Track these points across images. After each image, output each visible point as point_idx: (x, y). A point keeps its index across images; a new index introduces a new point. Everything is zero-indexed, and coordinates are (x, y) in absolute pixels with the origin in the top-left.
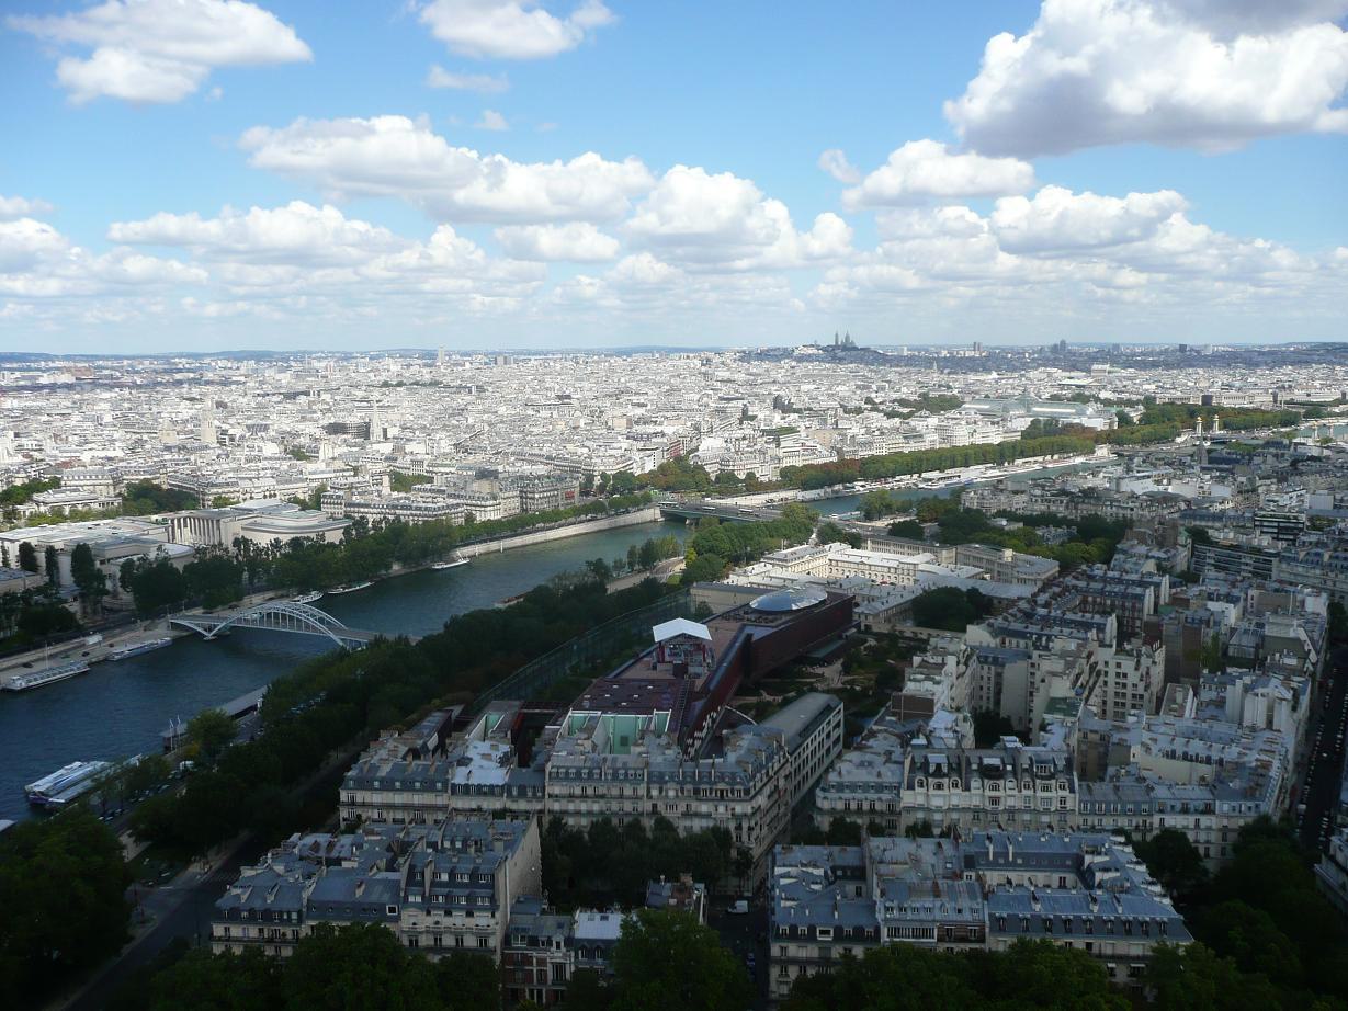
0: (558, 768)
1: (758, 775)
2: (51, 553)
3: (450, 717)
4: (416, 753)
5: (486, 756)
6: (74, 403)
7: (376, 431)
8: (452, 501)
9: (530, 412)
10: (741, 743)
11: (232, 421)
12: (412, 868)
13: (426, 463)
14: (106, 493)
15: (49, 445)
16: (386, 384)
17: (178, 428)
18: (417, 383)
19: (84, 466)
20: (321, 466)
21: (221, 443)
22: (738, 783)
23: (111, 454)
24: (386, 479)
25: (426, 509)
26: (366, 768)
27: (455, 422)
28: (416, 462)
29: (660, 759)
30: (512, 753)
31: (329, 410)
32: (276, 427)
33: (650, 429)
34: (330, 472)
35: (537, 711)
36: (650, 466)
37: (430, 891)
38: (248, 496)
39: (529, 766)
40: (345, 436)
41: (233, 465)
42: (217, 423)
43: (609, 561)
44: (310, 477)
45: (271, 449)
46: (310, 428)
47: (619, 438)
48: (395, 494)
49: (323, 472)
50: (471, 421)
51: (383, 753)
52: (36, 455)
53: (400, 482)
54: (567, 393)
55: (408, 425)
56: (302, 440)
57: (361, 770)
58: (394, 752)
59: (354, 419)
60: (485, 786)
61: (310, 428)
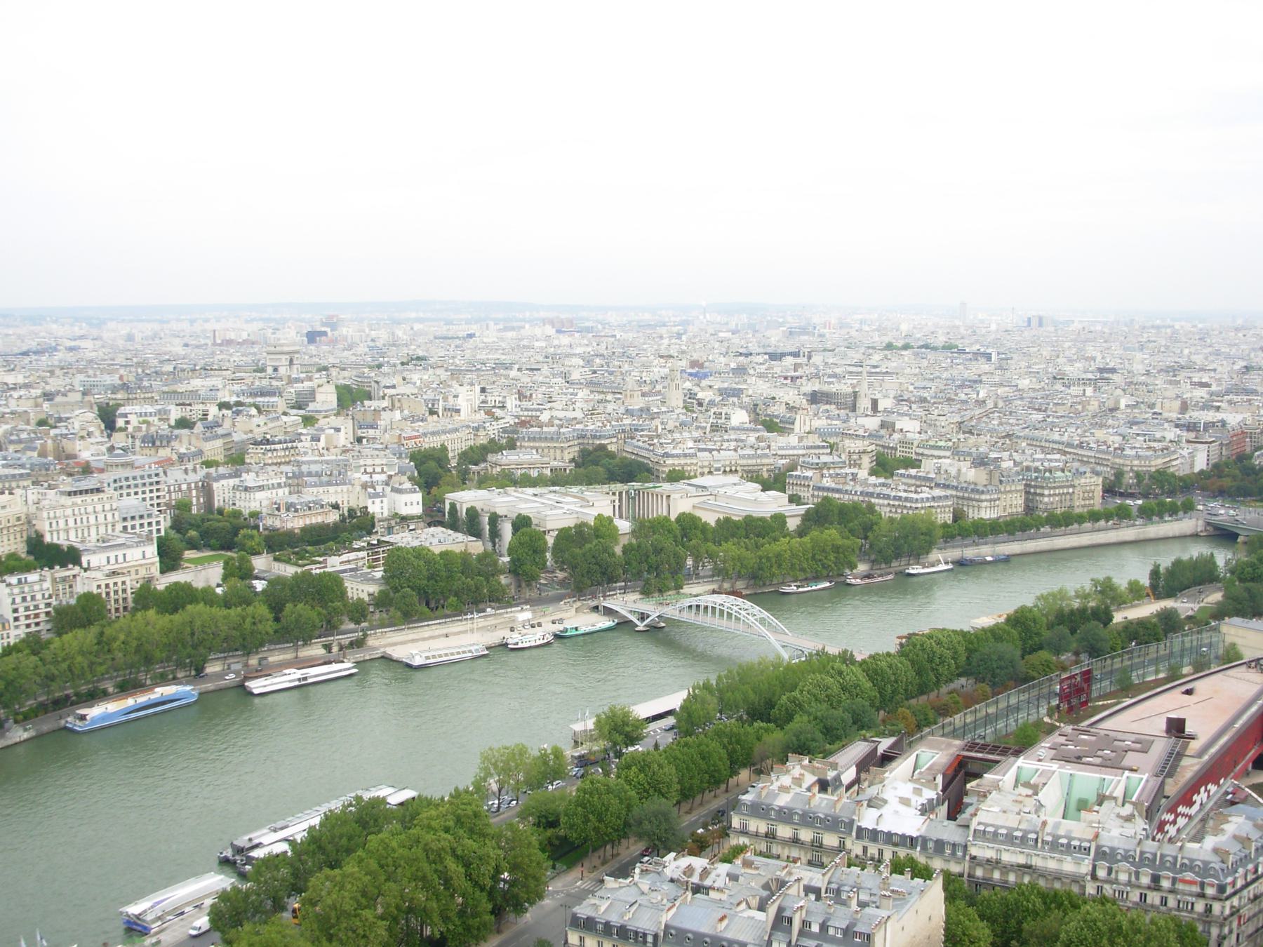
0: (986, 825)
1: (1241, 870)
2: (494, 519)
3: (876, 748)
4: (823, 785)
5: (905, 802)
6: (546, 357)
7: (864, 403)
8: (938, 492)
9: (1059, 387)
10: (1225, 826)
11: (704, 383)
12: (781, 910)
13: (916, 443)
14: (564, 458)
15: (512, 402)
16: (889, 346)
17: (646, 389)
18: (926, 346)
19: (541, 427)
20: (793, 440)
21: (688, 408)
22: (1211, 876)
23: (570, 415)
24: (866, 462)
25: (906, 499)
26: (764, 794)
27: (963, 397)
28: (907, 443)
29: (1115, 832)
30: (940, 802)
31: (817, 376)
32: (750, 392)
33: (1210, 416)
34: (800, 449)
35: (980, 755)
36: (1201, 463)
37: (797, 940)
38: (706, 470)
39: (955, 819)
40: (827, 407)
41: (696, 434)
42: (688, 385)
43: (1121, 582)
44: (780, 452)
45: (740, 417)
46: (789, 395)
47: (1166, 425)
48: (873, 479)
49: (794, 448)
50: (982, 395)
51: (786, 780)
52: (498, 412)
53: (884, 466)
54: (1111, 365)
55: (905, 398)
56: (778, 410)
57: (759, 794)
58: (798, 781)
59: (844, 387)
60: (896, 834)
61: (789, 395)
